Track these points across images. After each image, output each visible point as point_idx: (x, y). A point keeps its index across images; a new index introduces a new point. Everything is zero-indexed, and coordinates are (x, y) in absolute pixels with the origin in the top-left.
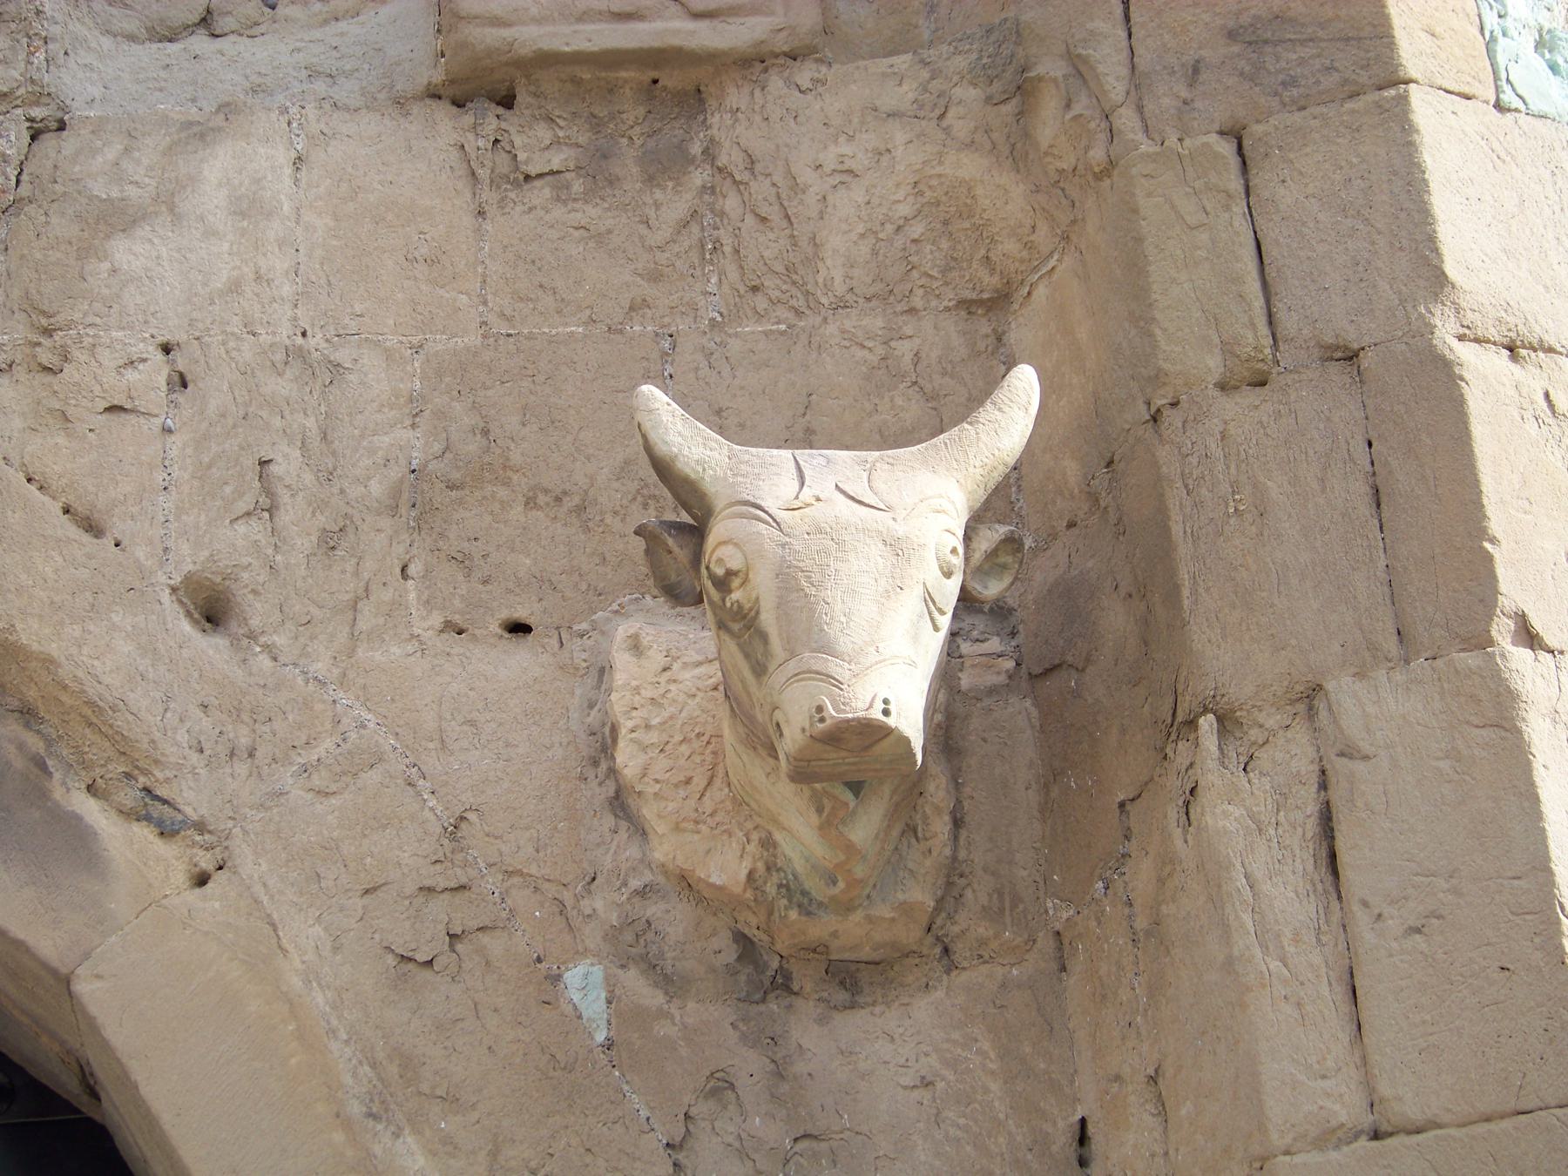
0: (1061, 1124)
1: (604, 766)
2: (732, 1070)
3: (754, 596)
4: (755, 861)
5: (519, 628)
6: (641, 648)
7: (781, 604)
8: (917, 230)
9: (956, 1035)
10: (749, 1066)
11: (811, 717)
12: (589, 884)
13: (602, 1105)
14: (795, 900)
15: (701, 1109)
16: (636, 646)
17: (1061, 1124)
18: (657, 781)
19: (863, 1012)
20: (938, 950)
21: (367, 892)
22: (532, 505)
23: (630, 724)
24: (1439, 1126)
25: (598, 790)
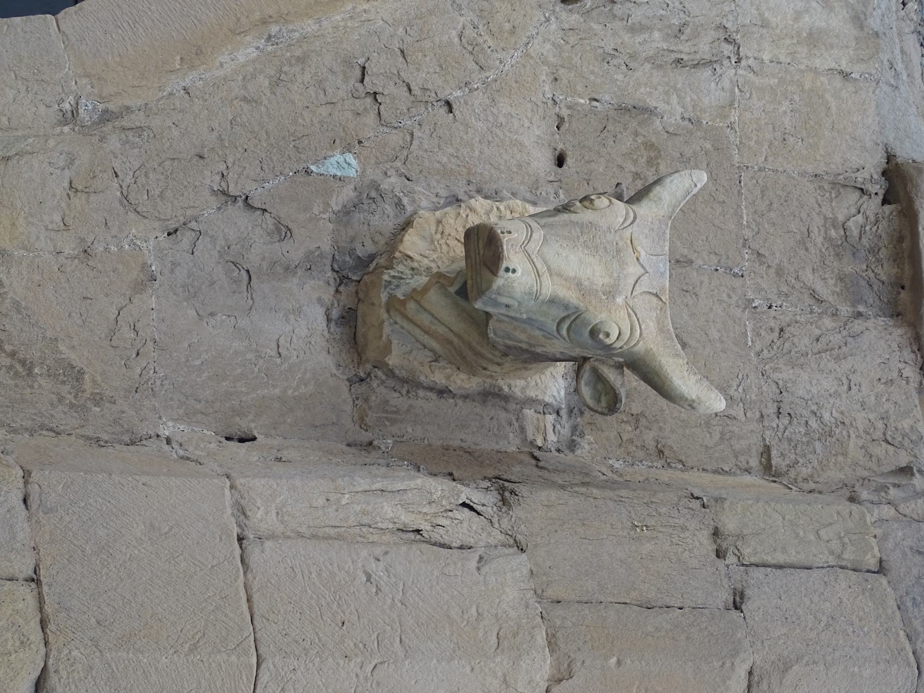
0: (252, 425)
2: (292, 240)
4: (418, 262)
5: (560, 161)
8: (813, 424)
9: (308, 375)
10: (295, 251)
12: (406, 176)
13: (272, 162)
14: (394, 280)
17: (252, 425)
18: (467, 216)
19: (325, 324)
20: (362, 374)
21: (402, 52)
22: (636, 177)
23: (502, 208)
24: (245, 573)
25: (462, 190)
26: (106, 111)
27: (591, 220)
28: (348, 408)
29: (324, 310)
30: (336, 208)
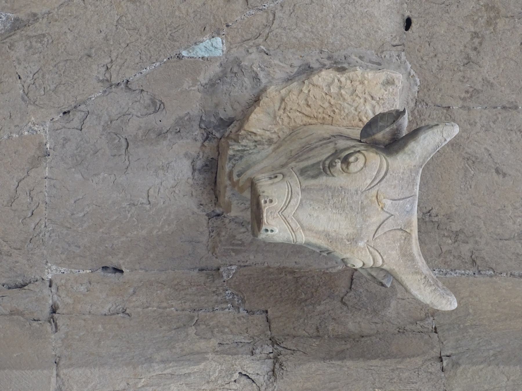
0: (121, 262)
1: (328, 63)
2: (164, 112)
3: (335, 174)
4: (260, 135)
5: (408, 23)
6: (386, 86)
7: (328, 188)
9: (172, 217)
11: (268, 197)
12: (265, 52)
13: (150, 52)
14: (238, 153)
15: (146, 98)
16: (389, 82)
17: (121, 262)
18: (309, 91)
19: (190, 174)
22: (474, 35)
23: (343, 79)
25: (314, 59)
26: (17, 20)
27: (342, 185)
28: (204, 239)
29: (191, 161)
30: (203, 82)
